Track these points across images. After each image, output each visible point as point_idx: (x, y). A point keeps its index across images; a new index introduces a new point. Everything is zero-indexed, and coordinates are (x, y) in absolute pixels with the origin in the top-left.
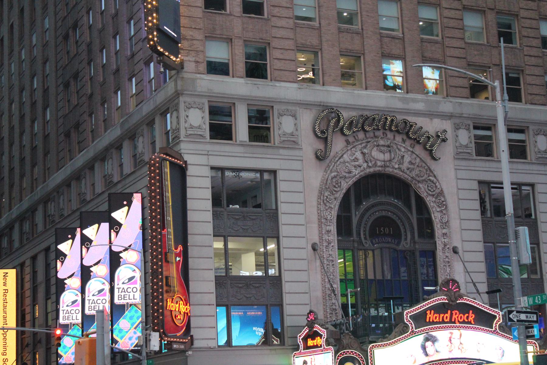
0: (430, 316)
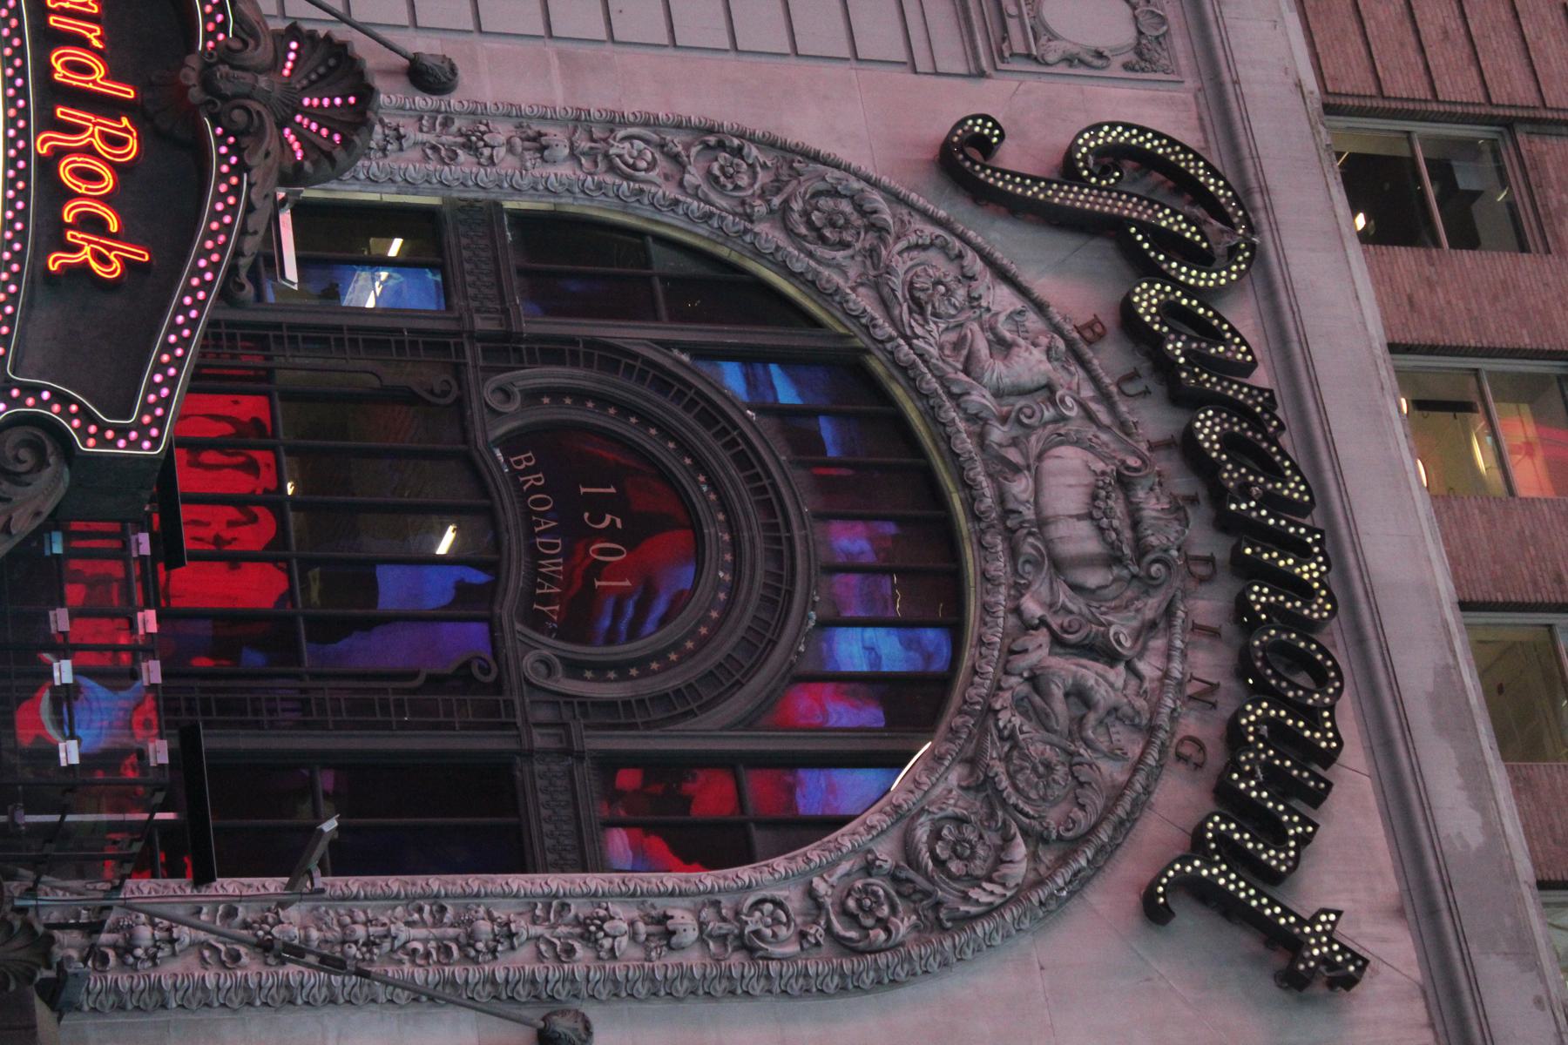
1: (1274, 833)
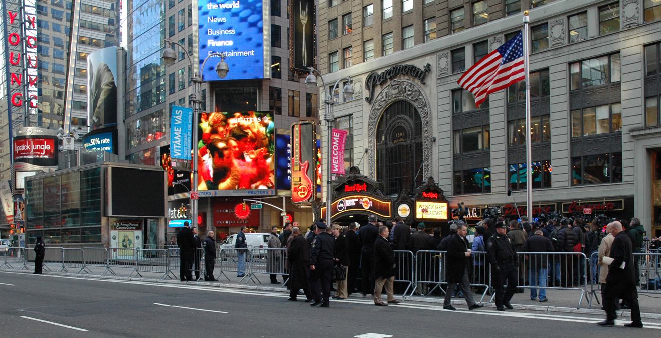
1: (418, 72)
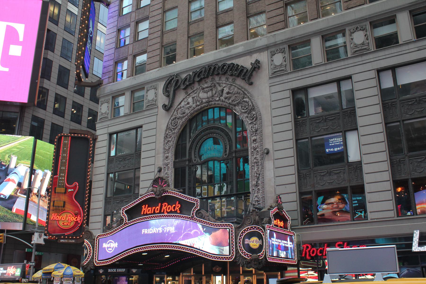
0: (145, 209)
1: (242, 71)
